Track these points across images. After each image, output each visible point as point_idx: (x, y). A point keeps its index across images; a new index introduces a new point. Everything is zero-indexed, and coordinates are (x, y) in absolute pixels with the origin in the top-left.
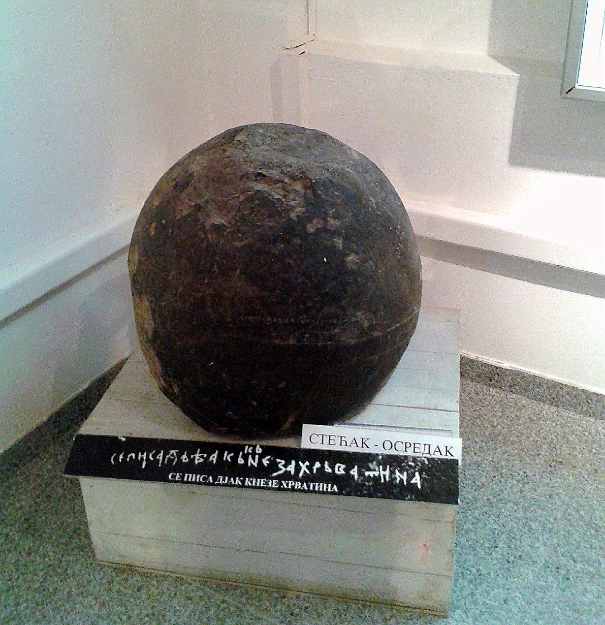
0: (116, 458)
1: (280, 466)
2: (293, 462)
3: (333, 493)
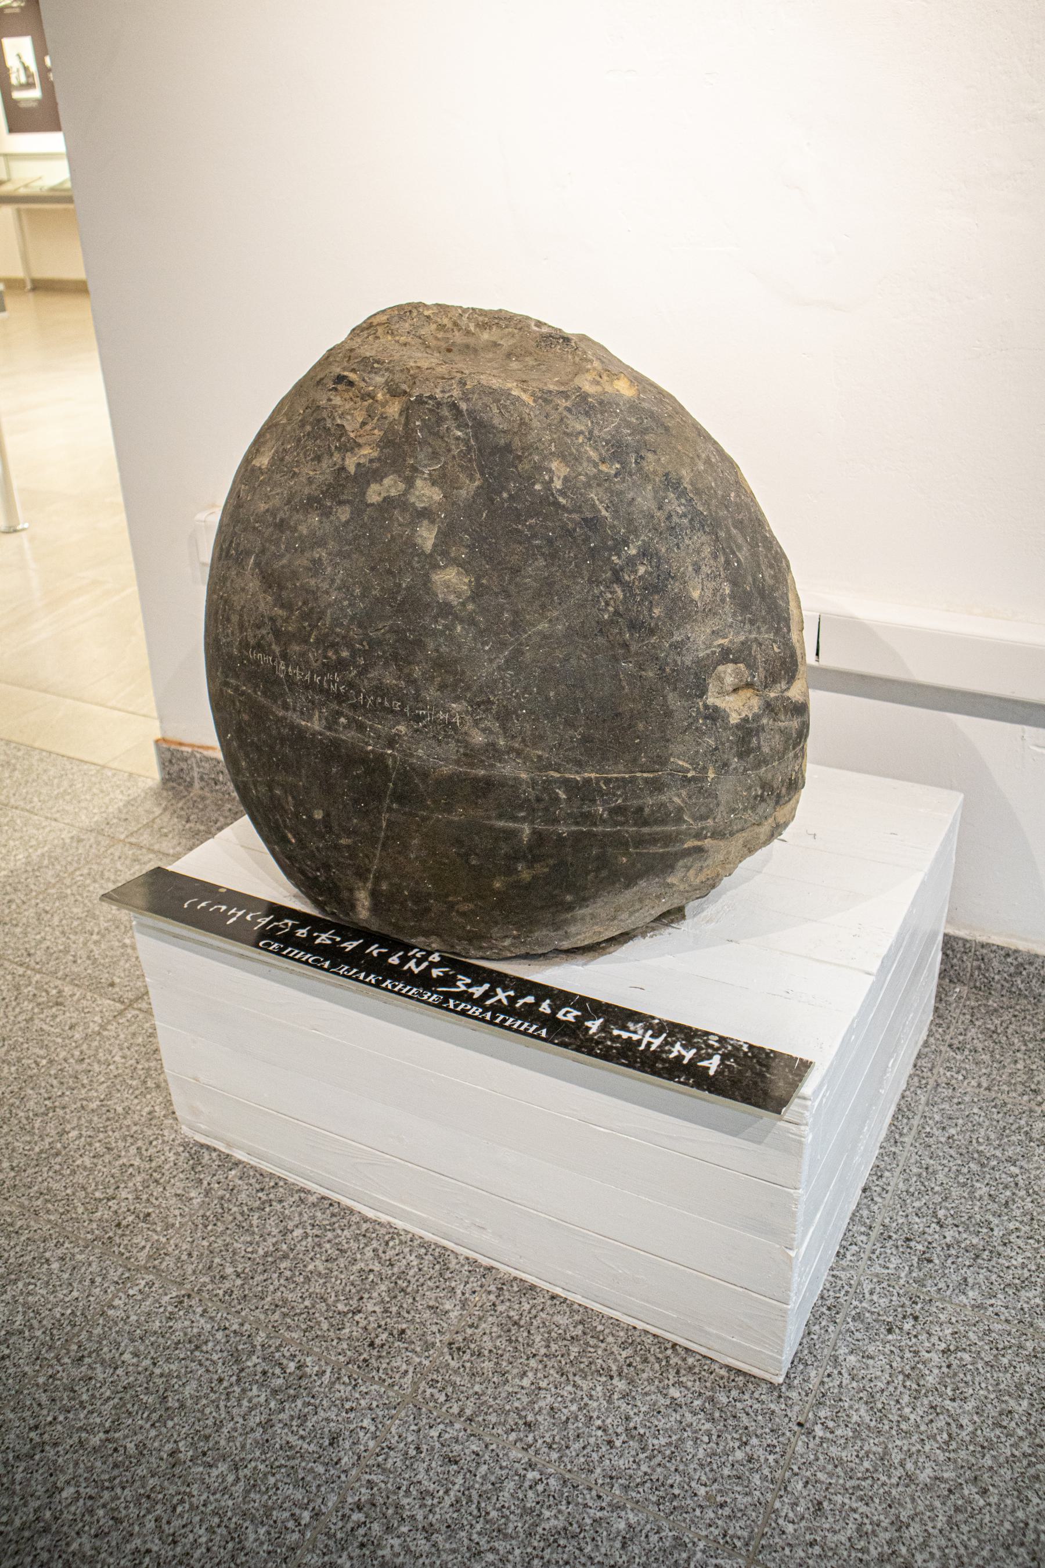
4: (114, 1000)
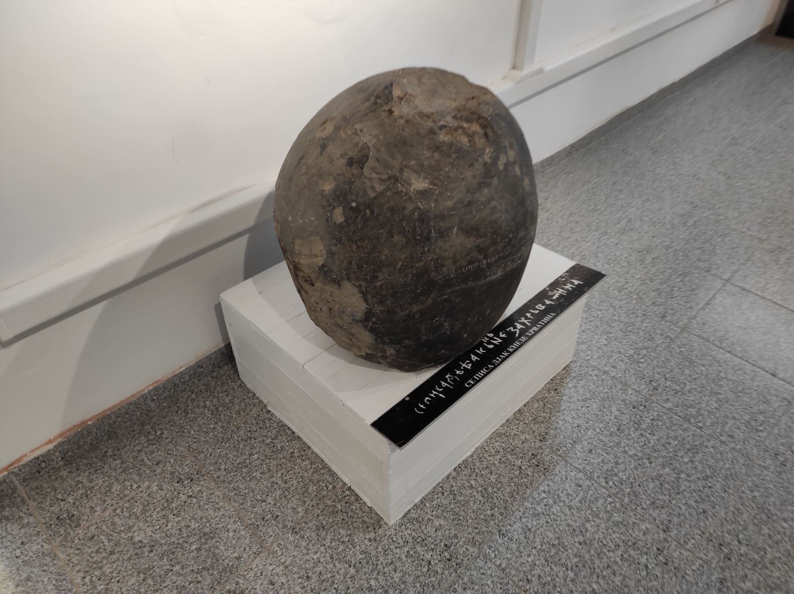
0: (420, 409)
1: (512, 330)
2: (516, 324)
3: (555, 317)
4: (255, 558)
